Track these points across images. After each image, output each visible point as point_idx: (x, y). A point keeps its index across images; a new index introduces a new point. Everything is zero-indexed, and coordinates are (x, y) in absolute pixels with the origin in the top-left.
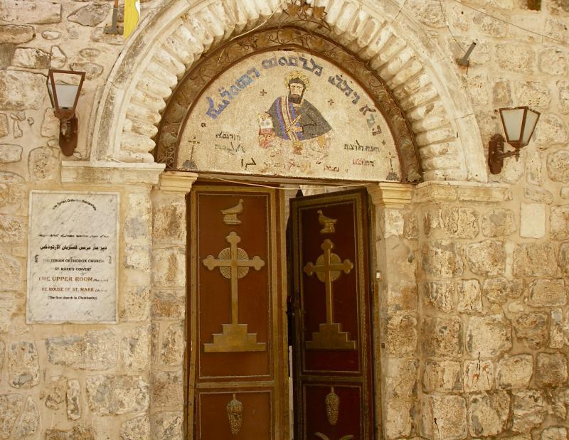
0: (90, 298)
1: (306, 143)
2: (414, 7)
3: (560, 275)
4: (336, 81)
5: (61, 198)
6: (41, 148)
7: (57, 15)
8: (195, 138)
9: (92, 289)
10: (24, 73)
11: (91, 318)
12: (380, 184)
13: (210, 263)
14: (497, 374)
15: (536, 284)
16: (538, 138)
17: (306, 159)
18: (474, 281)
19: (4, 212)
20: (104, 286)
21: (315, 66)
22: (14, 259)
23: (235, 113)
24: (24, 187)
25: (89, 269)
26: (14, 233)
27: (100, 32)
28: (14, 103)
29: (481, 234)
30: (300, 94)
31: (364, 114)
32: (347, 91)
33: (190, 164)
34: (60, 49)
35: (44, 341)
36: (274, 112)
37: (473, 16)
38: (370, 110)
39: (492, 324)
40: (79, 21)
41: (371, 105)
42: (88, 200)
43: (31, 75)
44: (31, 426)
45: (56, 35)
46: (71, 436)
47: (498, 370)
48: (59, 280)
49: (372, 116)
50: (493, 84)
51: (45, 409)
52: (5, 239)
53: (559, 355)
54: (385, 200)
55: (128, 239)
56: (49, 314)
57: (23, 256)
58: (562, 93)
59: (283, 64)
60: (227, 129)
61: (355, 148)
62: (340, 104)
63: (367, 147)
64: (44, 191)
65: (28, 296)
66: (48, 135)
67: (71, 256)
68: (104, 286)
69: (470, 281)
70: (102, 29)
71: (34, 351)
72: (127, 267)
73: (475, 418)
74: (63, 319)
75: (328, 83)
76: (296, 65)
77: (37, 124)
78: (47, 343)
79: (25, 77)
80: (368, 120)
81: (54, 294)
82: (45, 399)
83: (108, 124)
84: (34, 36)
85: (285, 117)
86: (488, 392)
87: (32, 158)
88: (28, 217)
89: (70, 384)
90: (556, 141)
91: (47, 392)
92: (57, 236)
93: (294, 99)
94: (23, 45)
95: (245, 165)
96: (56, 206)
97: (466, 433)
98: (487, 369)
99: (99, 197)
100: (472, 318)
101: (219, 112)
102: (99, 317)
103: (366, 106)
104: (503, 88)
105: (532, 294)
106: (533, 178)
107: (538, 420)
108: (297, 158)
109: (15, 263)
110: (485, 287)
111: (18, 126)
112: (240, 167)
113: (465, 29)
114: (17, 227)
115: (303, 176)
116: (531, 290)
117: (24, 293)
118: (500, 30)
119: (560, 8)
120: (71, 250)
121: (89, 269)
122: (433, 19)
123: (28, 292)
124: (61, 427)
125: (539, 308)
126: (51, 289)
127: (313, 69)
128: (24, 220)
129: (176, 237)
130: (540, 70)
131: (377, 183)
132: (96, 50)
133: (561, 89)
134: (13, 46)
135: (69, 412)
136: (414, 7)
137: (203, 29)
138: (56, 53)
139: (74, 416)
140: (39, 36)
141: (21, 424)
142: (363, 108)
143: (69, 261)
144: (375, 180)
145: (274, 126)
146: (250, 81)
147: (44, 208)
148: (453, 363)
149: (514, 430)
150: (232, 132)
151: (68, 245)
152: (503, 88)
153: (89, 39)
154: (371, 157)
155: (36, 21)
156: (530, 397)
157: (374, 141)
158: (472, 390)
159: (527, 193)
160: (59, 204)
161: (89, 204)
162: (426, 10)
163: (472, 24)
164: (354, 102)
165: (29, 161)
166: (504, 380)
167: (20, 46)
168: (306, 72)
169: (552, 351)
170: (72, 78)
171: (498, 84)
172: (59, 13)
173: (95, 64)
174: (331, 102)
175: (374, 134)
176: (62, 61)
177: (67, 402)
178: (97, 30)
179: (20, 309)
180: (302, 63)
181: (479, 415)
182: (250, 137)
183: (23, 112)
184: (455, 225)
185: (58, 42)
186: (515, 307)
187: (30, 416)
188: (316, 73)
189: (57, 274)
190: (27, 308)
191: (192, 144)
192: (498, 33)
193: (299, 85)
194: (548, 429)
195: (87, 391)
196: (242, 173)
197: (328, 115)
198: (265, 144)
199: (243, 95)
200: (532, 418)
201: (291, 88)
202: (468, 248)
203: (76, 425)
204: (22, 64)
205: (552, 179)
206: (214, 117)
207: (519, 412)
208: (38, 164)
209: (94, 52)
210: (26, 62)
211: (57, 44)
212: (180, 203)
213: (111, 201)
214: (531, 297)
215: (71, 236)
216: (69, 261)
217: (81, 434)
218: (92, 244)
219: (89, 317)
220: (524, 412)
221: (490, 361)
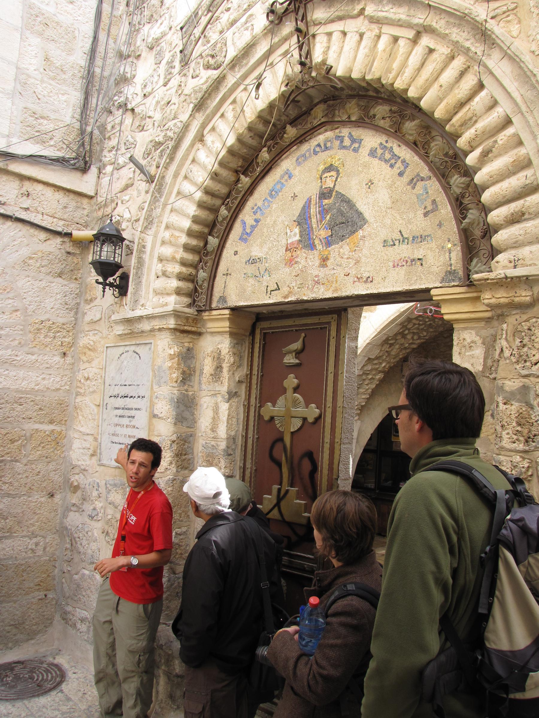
4: (380, 151)
7: (130, 178)
8: (228, 271)
12: (433, 292)
13: (269, 410)
17: (333, 272)
23: (265, 230)
30: (332, 186)
31: (413, 188)
32: (393, 161)
33: (223, 299)
35: (104, 482)
38: (422, 179)
41: (425, 171)
51: (105, 543)
55: (155, 387)
60: (256, 252)
61: (397, 243)
62: (380, 184)
63: (414, 238)
71: (100, 490)
72: (155, 416)
75: (367, 158)
78: (106, 484)
82: (105, 534)
83: (142, 273)
85: (314, 220)
101: (251, 232)
103: (418, 175)
108: (322, 273)
112: (265, 295)
115: (327, 296)
127: (351, 146)
129: (220, 383)
131: (428, 290)
137: (218, 145)
142: (413, 179)
143: (123, 409)
144: (423, 287)
145: (301, 236)
150: (260, 255)
160: (121, 355)
161: (137, 354)
164: (401, 174)
175: (426, 215)
180: (337, 143)
196: (266, 302)
198: (291, 261)
199: (274, 206)
212: (224, 345)
215: (125, 385)
216: (123, 409)
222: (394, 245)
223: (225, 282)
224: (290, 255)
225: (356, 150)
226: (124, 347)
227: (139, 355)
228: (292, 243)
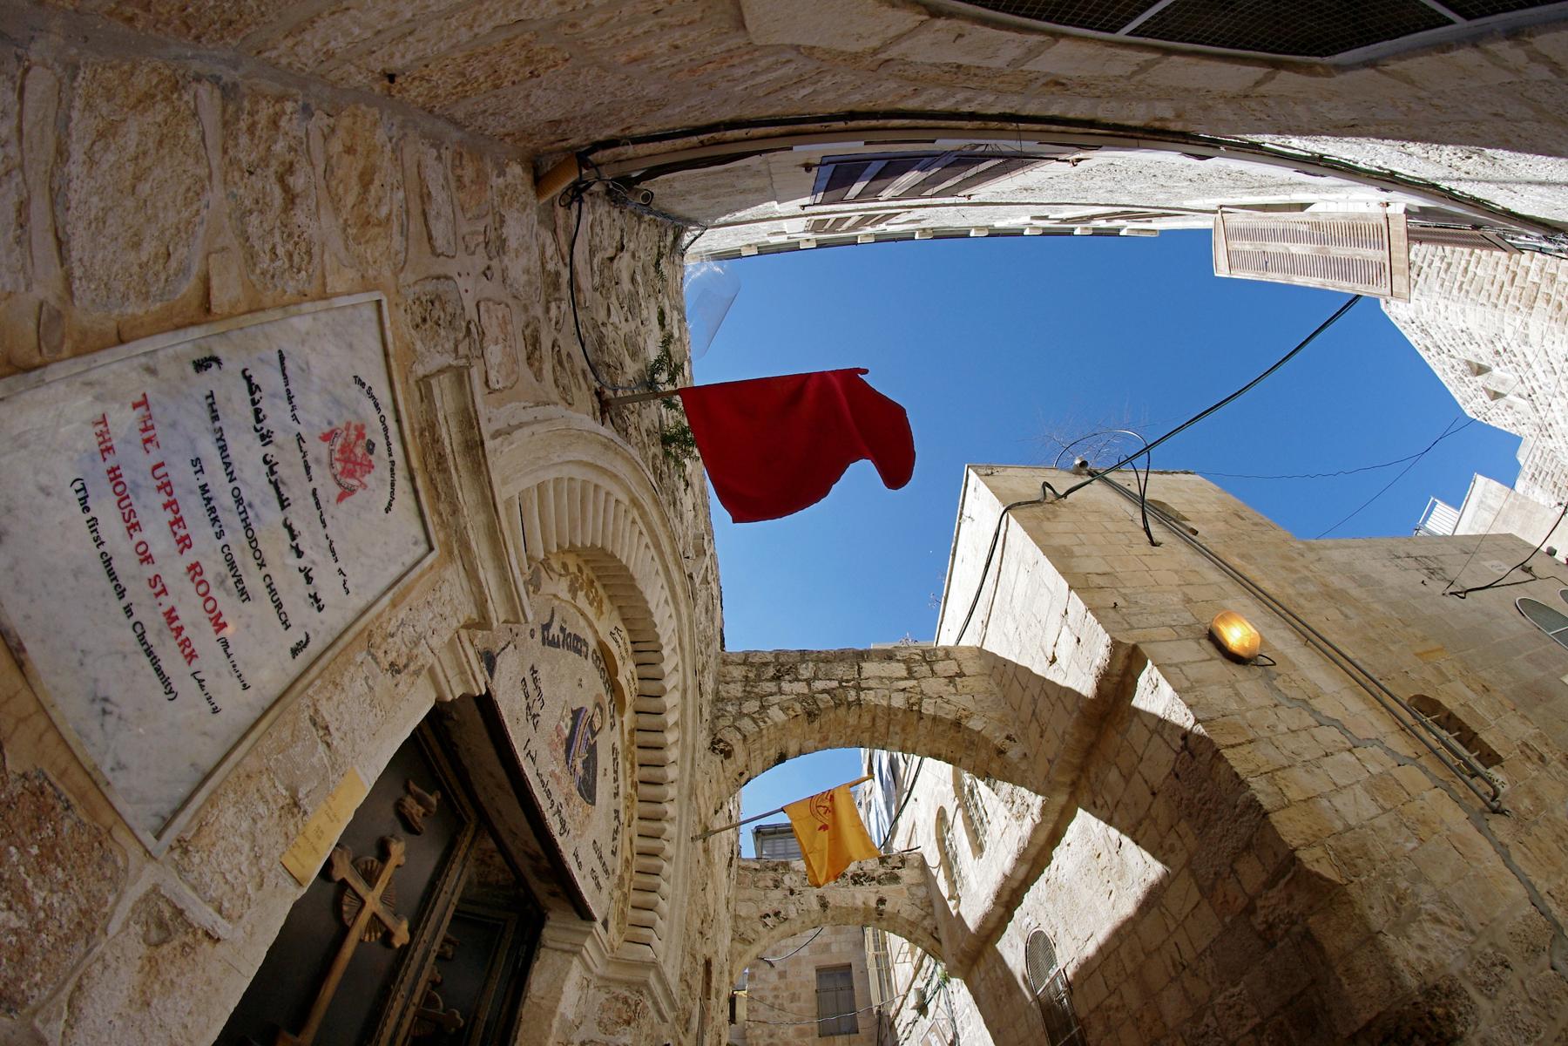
0: (158, 670)
6: (463, 309)
19: (322, 211)
22: (196, 268)
25: (244, 594)
26: (280, 251)
48: (164, 498)
52: (254, 220)
67: (257, 502)
81: (106, 509)
87: (443, 286)
88: (324, 296)
92: (295, 418)
102: (120, 766)
109: (184, 270)
114: (296, 258)
121: (244, 594)
126: (114, 474)
128: (314, 289)
143: (239, 501)
147: (351, 346)
161: (393, 485)
165: (438, 278)
189: (181, 474)
208: (437, 304)
216: (239, 501)
227: (393, 498)
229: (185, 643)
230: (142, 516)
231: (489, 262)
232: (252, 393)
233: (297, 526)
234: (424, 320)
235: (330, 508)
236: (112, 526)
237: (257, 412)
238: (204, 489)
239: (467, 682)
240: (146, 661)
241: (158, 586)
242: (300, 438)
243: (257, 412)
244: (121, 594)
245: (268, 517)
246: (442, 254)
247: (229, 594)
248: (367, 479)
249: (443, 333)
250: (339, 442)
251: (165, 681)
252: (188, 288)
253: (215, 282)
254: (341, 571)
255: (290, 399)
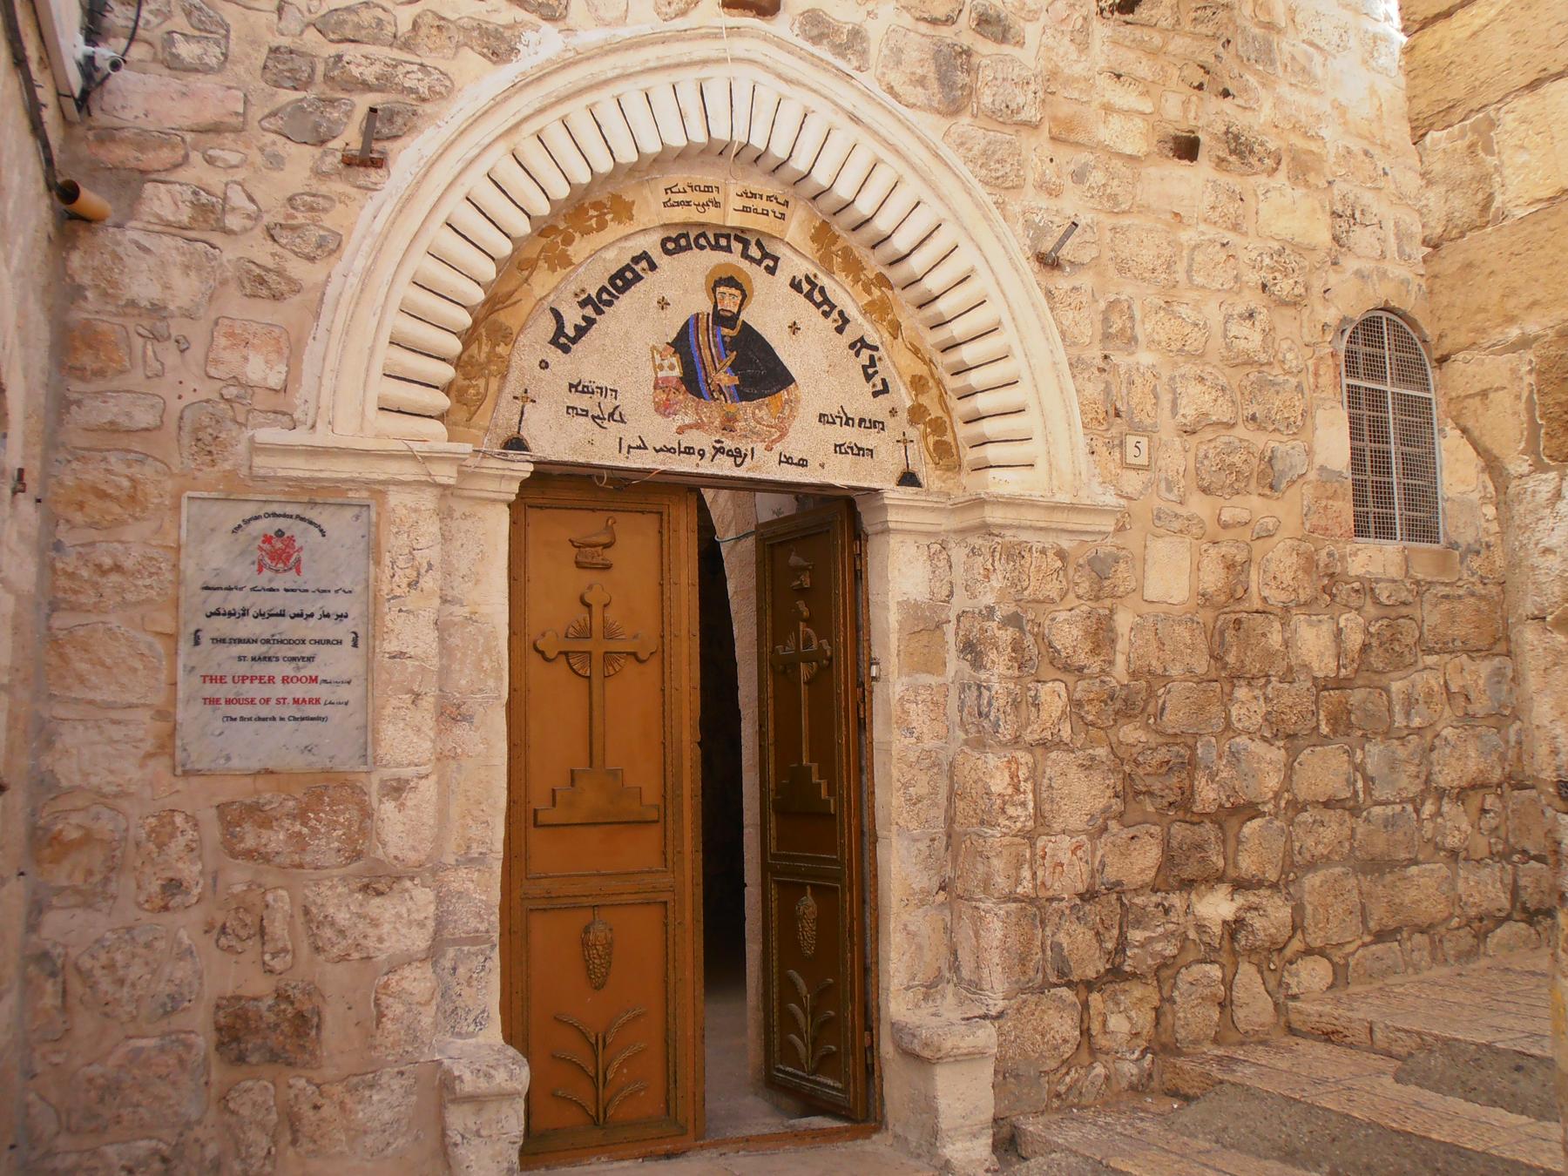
0: (312, 719)
1: (747, 407)
2: (962, 144)
3: (1213, 675)
5: (249, 510)
6: (207, 401)
7: (237, 114)
8: (526, 392)
9: (318, 701)
10: (166, 239)
11: (314, 759)
14: (1097, 863)
15: (1169, 692)
16: (1182, 411)
18: (1057, 683)
20: (343, 693)
21: (766, 255)
22: (149, 638)
24: (169, 485)
25: (310, 659)
26: (148, 582)
27: (333, 161)
28: (144, 303)
29: (1071, 596)
31: (857, 354)
32: (826, 308)
34: (244, 191)
36: (682, 344)
37: (1072, 167)
39: (1089, 766)
40: (287, 132)
42: (310, 514)
43: (181, 242)
44: (186, 990)
45: (234, 158)
46: (270, 1008)
47: (1099, 854)
48: (248, 682)
49: (872, 358)
50: (1102, 305)
51: (217, 953)
52: (129, 596)
53: (1208, 825)
54: (891, 525)
56: (224, 753)
57: (168, 631)
58: (1229, 325)
59: (702, 248)
61: (838, 420)
63: (862, 420)
64: (214, 495)
65: (180, 716)
66: (224, 376)
67: (274, 631)
68: (343, 693)
69: (1050, 684)
70: (339, 155)
73: (1057, 947)
74: (255, 765)
76: (728, 249)
77: (196, 352)
79: (167, 245)
80: (865, 368)
81: (238, 710)
82: (215, 932)
84: (186, 157)
86: (1081, 896)
87: (187, 427)
88: (178, 549)
89: (270, 897)
90: (1214, 418)
91: (220, 917)
92: (241, 589)
93: (721, 319)
94: (163, 176)
95: (625, 450)
96: (240, 526)
97: (1040, 976)
98: (1079, 853)
99: (332, 508)
100: (1053, 755)
103: (862, 340)
104: (1121, 311)
105: (1163, 709)
106: (1169, 490)
107: (1171, 950)
109: (150, 646)
110: (1077, 696)
111: (154, 352)
113: (1054, 192)
114: (153, 570)
116: (1160, 702)
117: (171, 710)
118: (1120, 199)
119: (1233, 158)
120: (273, 619)
121: (310, 659)
122: (996, 170)
123: (180, 706)
124: (247, 991)
125: (1176, 735)
126: (229, 702)
130: (1190, 279)
132: (324, 197)
133: (1228, 318)
134: (137, 175)
135: (267, 957)
136: (962, 144)
138: (237, 198)
139: (277, 964)
140: (196, 157)
141: (163, 988)
143: (267, 641)
146: (638, 278)
148: (1017, 840)
149: (1127, 969)
151: (265, 609)
152: (1121, 311)
153: (308, 173)
154: (867, 439)
155: (187, 123)
156: (1157, 905)
157: (876, 408)
158: (1050, 893)
159: (1159, 518)
160: (247, 522)
161: (311, 523)
162: (984, 153)
163: (1068, 182)
164: (840, 330)
165: (180, 428)
166: (1111, 874)
167: (154, 176)
168: (745, 265)
169: (1195, 819)
170: (274, 255)
171: (1112, 305)
172: (241, 110)
173: (321, 227)
174: (794, 328)
176: (249, 216)
177: (262, 937)
178: (325, 154)
179: (162, 747)
180: (740, 246)
181: (1062, 938)
182: (636, 395)
183: (164, 324)
184: (1025, 577)
185: (240, 175)
186: (1131, 733)
187: (182, 971)
188: (767, 268)
189: (243, 668)
190: (178, 743)
191: (520, 403)
192: (1117, 204)
193: (733, 291)
194: (1188, 966)
195: (307, 912)
196: (621, 465)
197: (787, 352)
200: (1158, 947)
201: (718, 296)
202: (1047, 622)
203: (282, 984)
204: (159, 217)
205: (1204, 491)
206: (566, 349)
207: (1136, 935)
208: (201, 435)
209: (321, 200)
210: (168, 213)
211: (238, 178)
213: (357, 517)
214: (1161, 714)
215: (272, 590)
216: (267, 641)
217: (292, 1003)
218: (319, 605)
219: (311, 758)
220: (1147, 934)
221: (1084, 837)
222: (834, 423)
223: (522, 413)
224: (664, 396)
225: (771, 271)
226: (261, 504)
227: (318, 526)
228: (666, 379)
229: (311, 701)
230: (250, 696)
231: (172, 341)
232: (219, 614)
233: (297, 611)
234: (210, 452)
235: (299, 582)
236: (245, 710)
237: (231, 614)
238: (253, 659)
239: (512, 478)
240: (305, 722)
241: (281, 701)
242: (253, 589)
243: (231, 614)
244: (274, 719)
245: (285, 626)
246: (161, 417)
247: (304, 667)
248: (297, 545)
249: (223, 435)
250: (267, 560)
251: (318, 719)
252: (159, 646)
253: (159, 629)
254: (337, 591)
255: (230, 589)
